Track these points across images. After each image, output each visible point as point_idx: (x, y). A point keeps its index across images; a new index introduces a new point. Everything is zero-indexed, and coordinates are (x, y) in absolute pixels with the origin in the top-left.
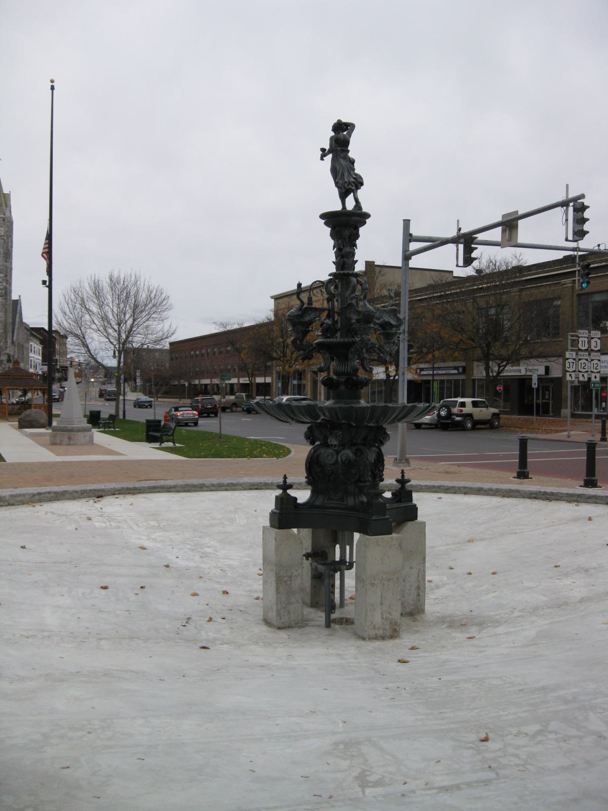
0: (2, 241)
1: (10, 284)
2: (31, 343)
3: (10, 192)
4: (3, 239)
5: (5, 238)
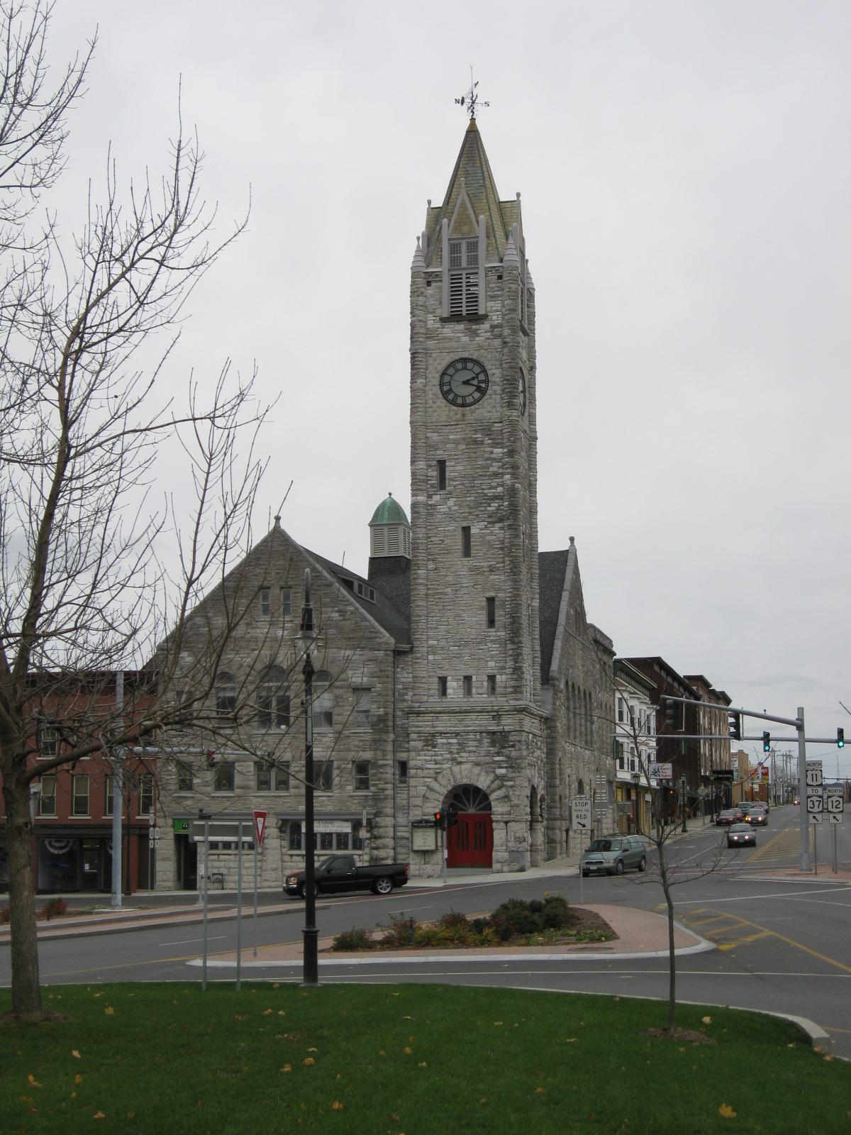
0: (497, 342)
1: (531, 487)
2: (618, 695)
3: (518, 195)
4: (500, 336)
5: (507, 332)
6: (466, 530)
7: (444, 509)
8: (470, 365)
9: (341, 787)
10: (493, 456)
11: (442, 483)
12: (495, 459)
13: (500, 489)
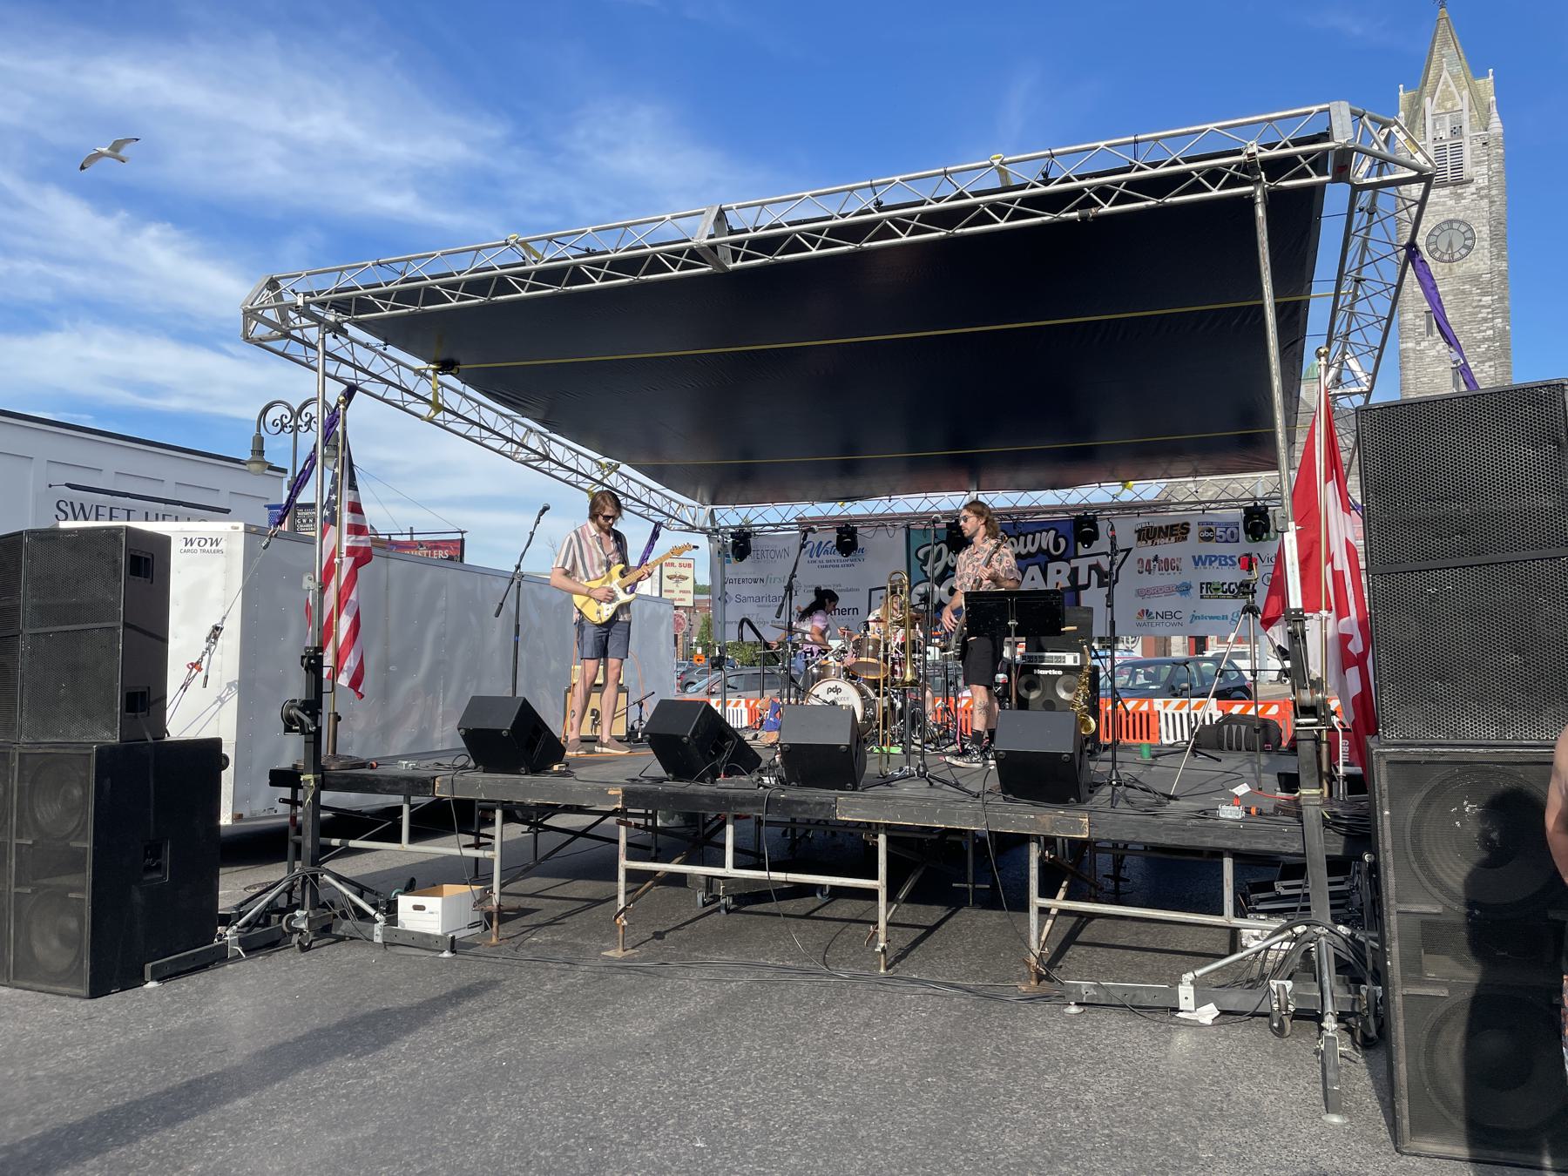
0: (1485, 203)
7: (1433, 353)
8: (1455, 226)
10: (1481, 303)
12: (1483, 306)
13: (1490, 332)
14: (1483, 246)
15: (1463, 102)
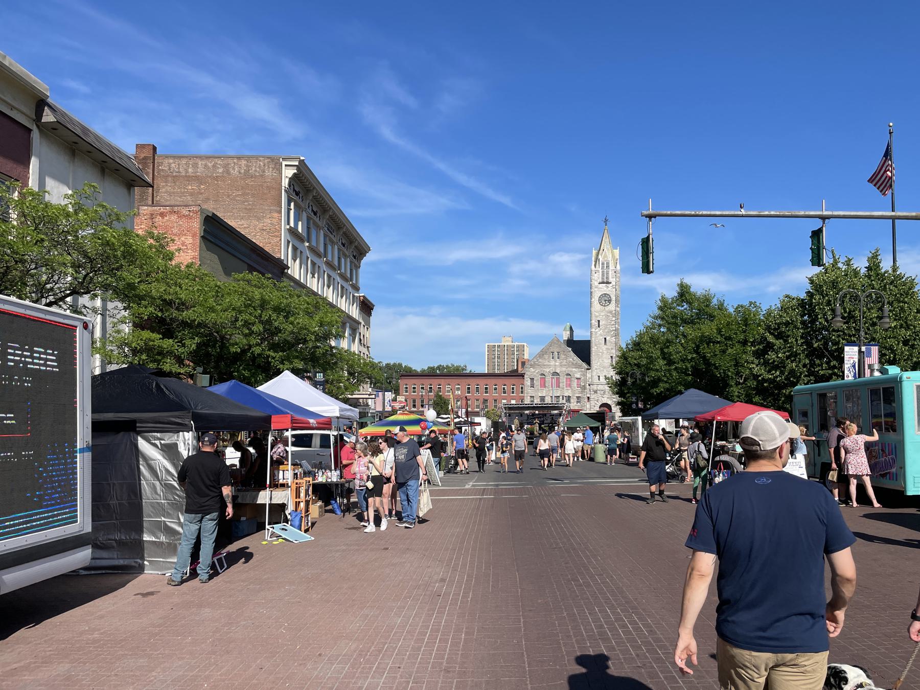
6: (605, 339)
9: (573, 403)
11: (599, 326)
14: (613, 302)
15: (610, 259)
